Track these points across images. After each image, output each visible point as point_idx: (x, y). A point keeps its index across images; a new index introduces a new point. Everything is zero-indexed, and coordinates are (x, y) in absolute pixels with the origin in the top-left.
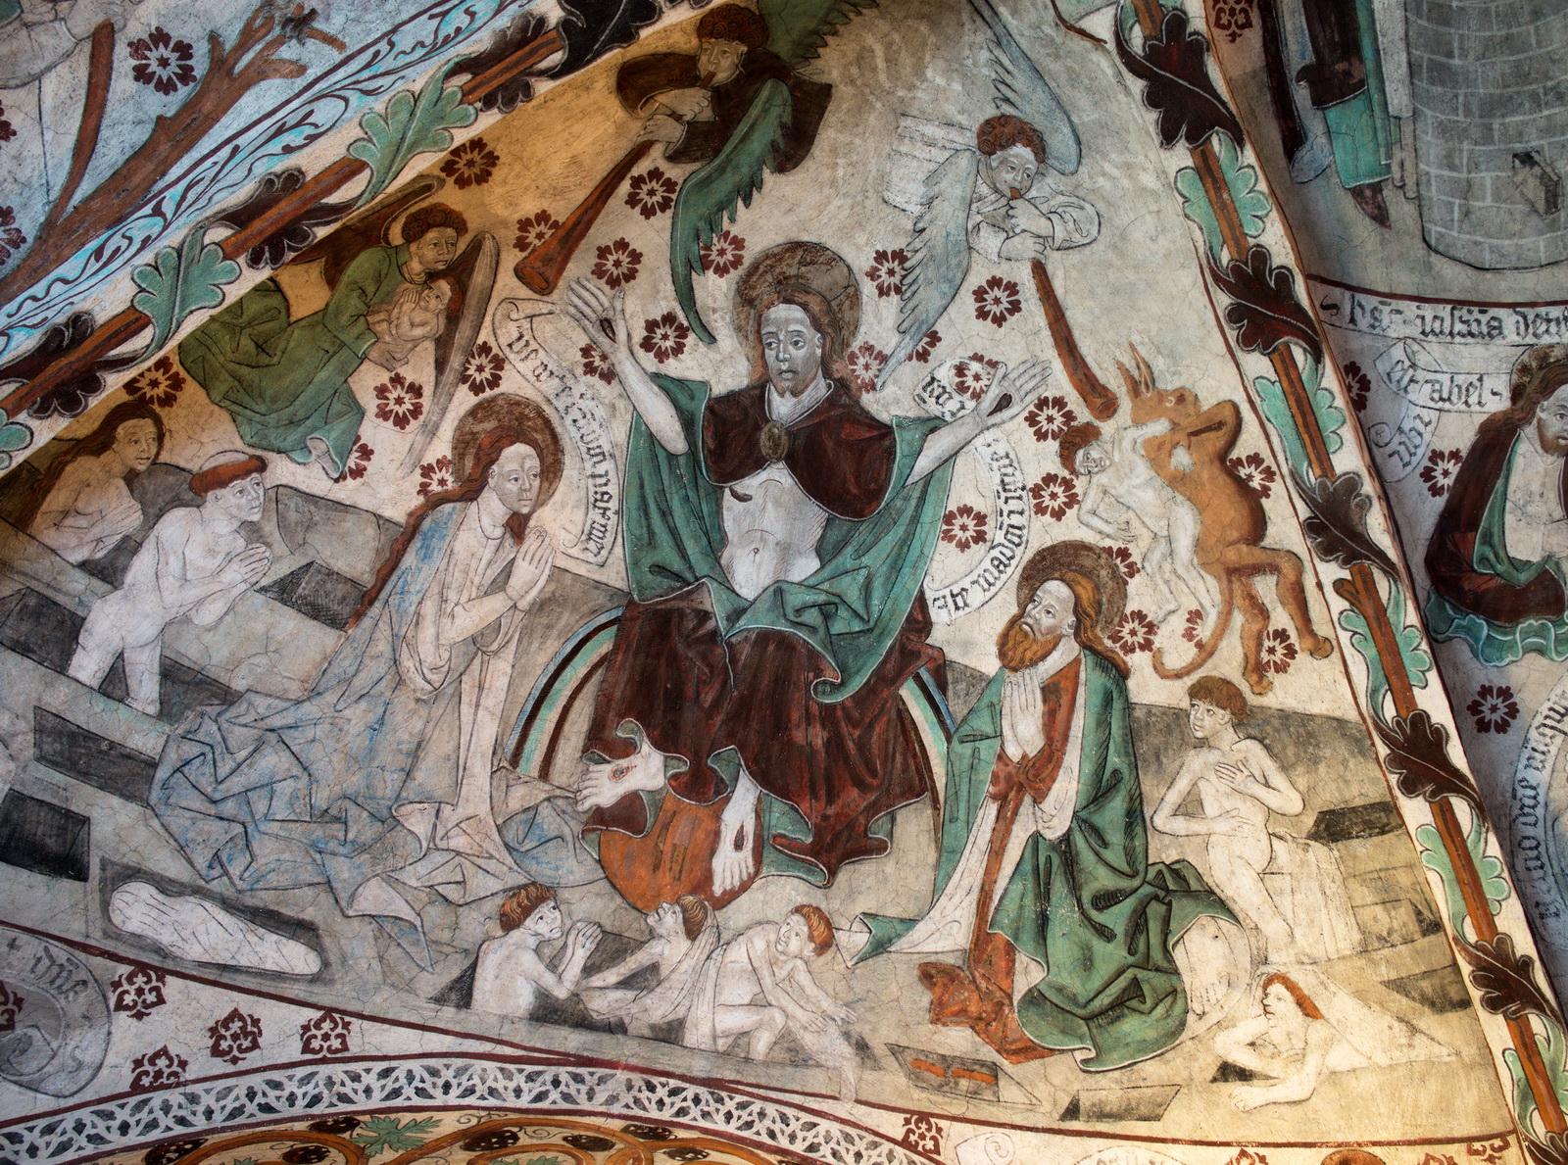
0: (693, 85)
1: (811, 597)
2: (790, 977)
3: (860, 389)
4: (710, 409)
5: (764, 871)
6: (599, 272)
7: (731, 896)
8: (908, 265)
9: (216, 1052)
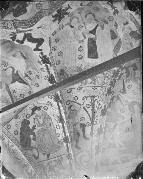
6: (129, 89)
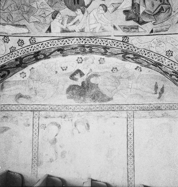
7: (88, 6)
9: (19, 45)
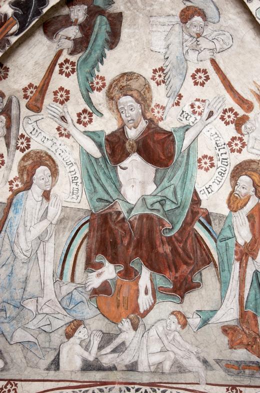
0: (71, 25)
1: (155, 199)
2: (174, 339)
3: (157, 121)
4: (106, 139)
5: (157, 301)
6: (56, 100)
7: (147, 312)
8: (165, 72)
